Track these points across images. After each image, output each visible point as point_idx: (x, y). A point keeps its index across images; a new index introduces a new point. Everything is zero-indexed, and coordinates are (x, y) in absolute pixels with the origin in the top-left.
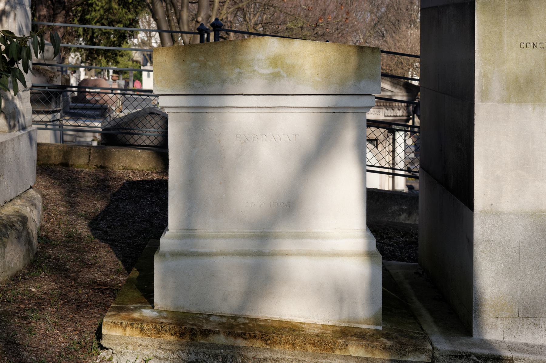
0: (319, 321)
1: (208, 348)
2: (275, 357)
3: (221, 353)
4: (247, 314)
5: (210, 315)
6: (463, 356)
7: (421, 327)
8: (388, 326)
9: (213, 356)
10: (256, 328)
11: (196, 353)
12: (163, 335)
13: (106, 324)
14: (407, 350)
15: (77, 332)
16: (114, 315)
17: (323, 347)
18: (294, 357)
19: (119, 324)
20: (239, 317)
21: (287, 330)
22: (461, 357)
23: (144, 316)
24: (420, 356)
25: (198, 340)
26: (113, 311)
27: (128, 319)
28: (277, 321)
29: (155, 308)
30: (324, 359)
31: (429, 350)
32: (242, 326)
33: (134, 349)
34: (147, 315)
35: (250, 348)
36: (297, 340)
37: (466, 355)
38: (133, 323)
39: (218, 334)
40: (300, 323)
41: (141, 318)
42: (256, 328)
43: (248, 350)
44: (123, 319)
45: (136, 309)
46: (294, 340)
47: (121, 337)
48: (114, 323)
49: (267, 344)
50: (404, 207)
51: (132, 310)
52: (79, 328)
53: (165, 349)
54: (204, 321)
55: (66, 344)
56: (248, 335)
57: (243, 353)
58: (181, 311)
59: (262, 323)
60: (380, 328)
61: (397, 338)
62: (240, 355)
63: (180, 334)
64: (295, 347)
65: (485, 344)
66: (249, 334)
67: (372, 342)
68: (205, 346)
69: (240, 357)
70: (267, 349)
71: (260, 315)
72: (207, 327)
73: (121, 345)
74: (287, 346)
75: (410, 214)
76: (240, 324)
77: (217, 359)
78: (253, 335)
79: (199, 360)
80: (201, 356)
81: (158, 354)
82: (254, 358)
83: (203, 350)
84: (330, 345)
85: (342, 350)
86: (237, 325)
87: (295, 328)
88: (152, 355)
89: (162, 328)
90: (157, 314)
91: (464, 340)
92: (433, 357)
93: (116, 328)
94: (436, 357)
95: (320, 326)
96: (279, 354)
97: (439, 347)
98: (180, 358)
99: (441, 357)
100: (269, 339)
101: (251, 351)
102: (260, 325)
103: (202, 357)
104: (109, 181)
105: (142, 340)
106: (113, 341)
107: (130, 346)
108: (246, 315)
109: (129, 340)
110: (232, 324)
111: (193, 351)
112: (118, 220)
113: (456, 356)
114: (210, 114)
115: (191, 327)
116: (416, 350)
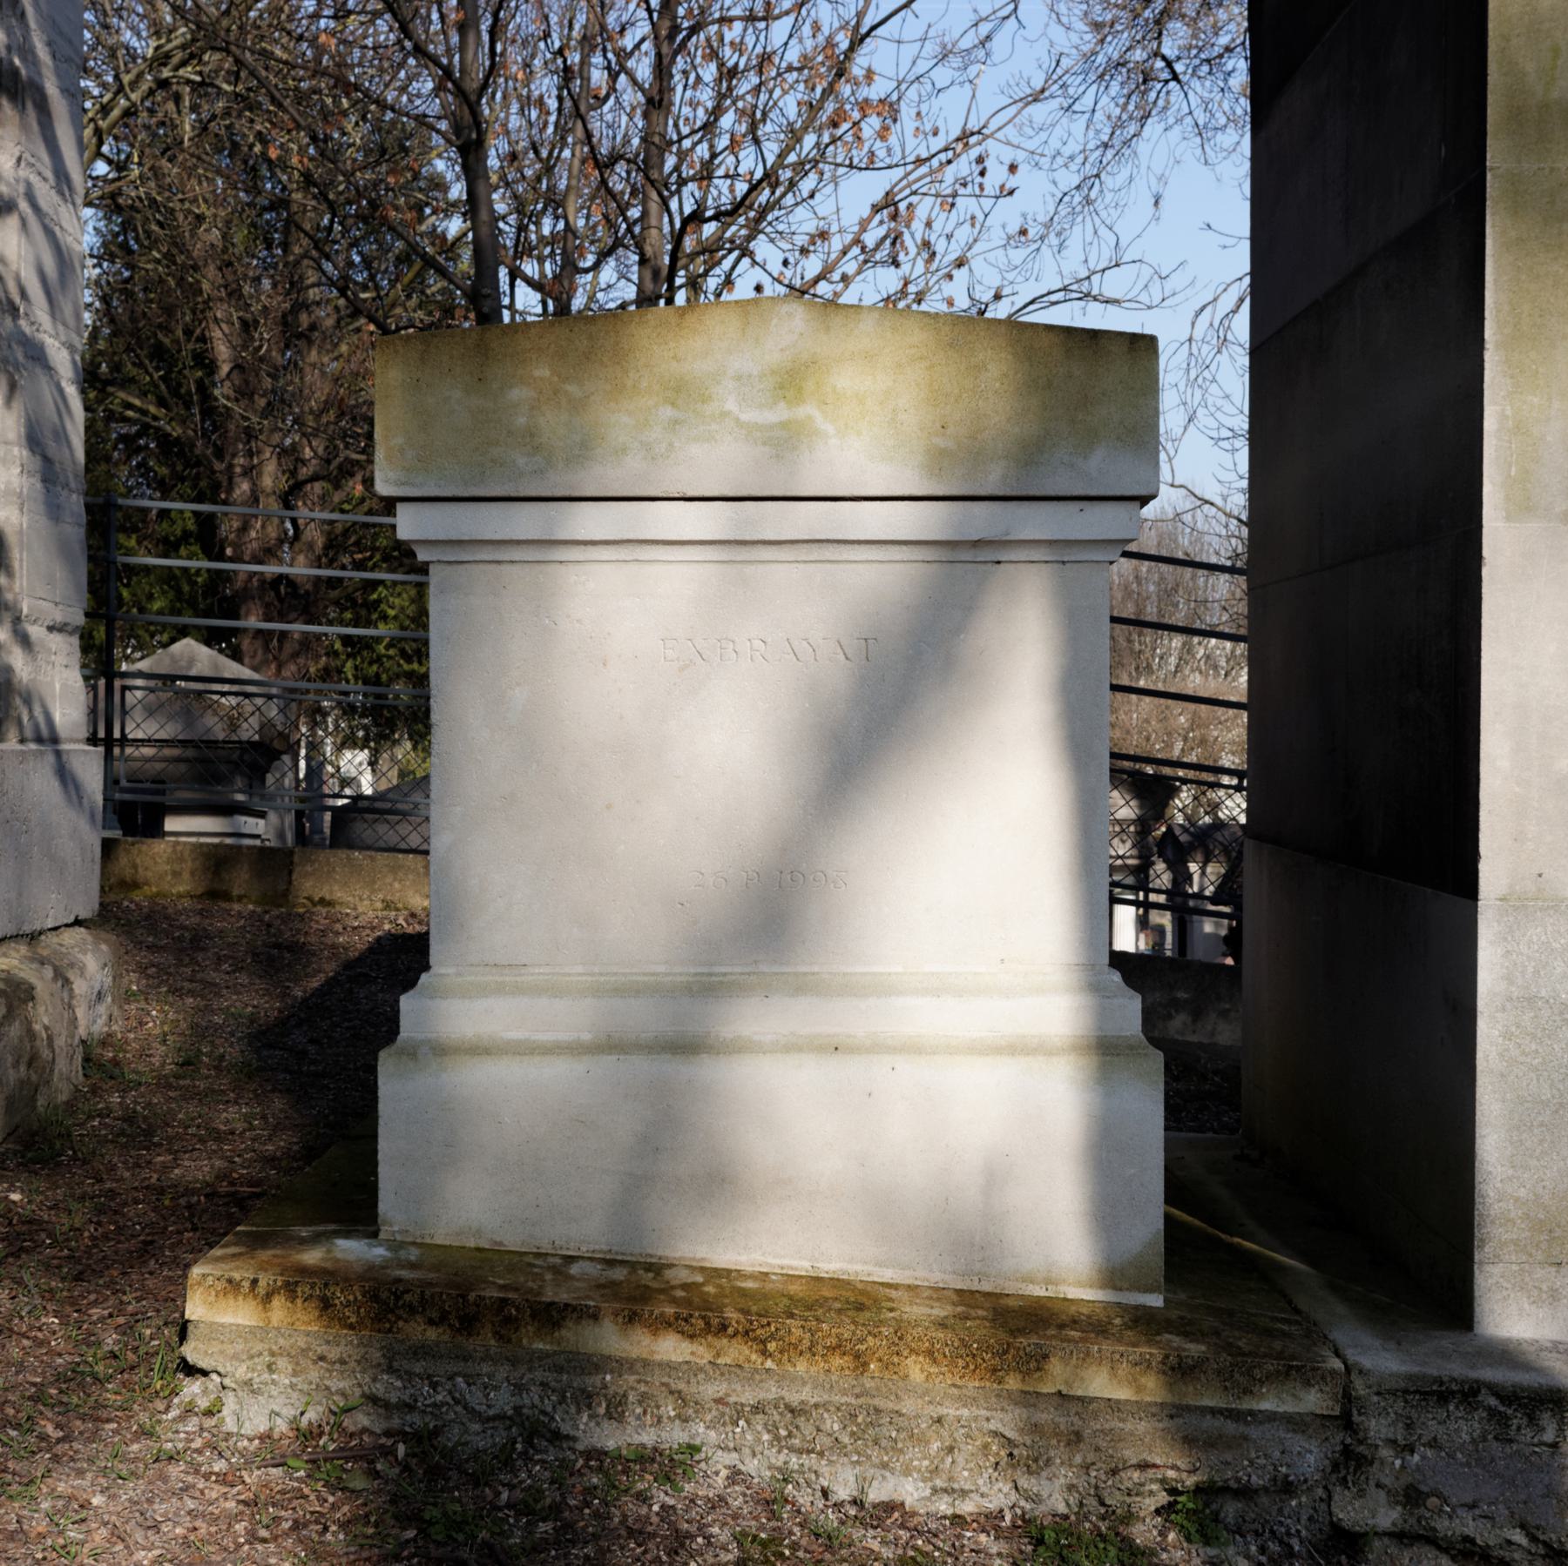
1: (560, 1369)
2: (794, 1398)
3: (605, 1387)
4: (699, 1255)
5: (570, 1259)
6: (1453, 1393)
7: (1290, 1302)
8: (1183, 1296)
10: (727, 1301)
11: (515, 1385)
12: (401, 1324)
13: (199, 1284)
14: (1257, 1373)
15: (121, 1320)
16: (234, 1255)
17: (961, 1363)
18: (861, 1401)
19: (246, 1284)
20: (671, 1266)
21: (837, 1305)
22: (1443, 1397)
23: (338, 1260)
24: (1302, 1394)
25: (525, 1341)
26: (236, 1244)
27: (278, 1270)
29: (382, 1236)
30: (965, 1406)
31: (1333, 1372)
32: (680, 1293)
33: (295, 1374)
34: (351, 1257)
35: (708, 1367)
36: (870, 1338)
37: (1462, 1392)
38: (297, 1283)
39: (595, 1317)
40: (882, 1284)
41: (328, 1265)
42: (727, 1301)
43: (701, 1376)
44: (262, 1268)
45: (315, 1239)
46: (862, 1341)
47: (252, 1330)
48: (230, 1281)
49: (765, 1353)
50: (1182, 995)
51: (303, 1242)
52: (130, 1308)
53: (406, 1372)
54: (549, 1277)
55: (68, 1358)
56: (701, 1323)
57: (681, 1386)
58: (472, 1245)
59: (750, 1284)
60: (1155, 1301)
61: (1217, 1333)
62: (672, 1393)
64: (865, 1365)
65: (1505, 1354)
66: (703, 1318)
70: (767, 1370)
71: (743, 1258)
72: (556, 1294)
73: (251, 1357)
74: (837, 1361)
75: (1197, 1014)
76: (673, 1288)
77: (589, 1407)
79: (525, 1411)
81: (379, 1389)
82: (718, 1401)
83: (539, 1375)
86: (662, 1291)
87: (864, 1300)
88: (358, 1392)
89: (398, 1298)
91: (1447, 1340)
92: (1347, 1398)
94: (1358, 1398)
95: (950, 1293)
96: (807, 1389)
97: (1366, 1362)
98: (457, 1402)
99: (1375, 1399)
100: (772, 1337)
101: (708, 1379)
102: (743, 1289)
104: (337, 934)
105: (328, 1342)
106: (225, 1346)
107: (282, 1363)
109: (282, 1341)
110: (647, 1287)
111: (507, 1379)
112: (348, 1028)
113: (1425, 1395)
115: (501, 1295)
116: (1287, 1374)
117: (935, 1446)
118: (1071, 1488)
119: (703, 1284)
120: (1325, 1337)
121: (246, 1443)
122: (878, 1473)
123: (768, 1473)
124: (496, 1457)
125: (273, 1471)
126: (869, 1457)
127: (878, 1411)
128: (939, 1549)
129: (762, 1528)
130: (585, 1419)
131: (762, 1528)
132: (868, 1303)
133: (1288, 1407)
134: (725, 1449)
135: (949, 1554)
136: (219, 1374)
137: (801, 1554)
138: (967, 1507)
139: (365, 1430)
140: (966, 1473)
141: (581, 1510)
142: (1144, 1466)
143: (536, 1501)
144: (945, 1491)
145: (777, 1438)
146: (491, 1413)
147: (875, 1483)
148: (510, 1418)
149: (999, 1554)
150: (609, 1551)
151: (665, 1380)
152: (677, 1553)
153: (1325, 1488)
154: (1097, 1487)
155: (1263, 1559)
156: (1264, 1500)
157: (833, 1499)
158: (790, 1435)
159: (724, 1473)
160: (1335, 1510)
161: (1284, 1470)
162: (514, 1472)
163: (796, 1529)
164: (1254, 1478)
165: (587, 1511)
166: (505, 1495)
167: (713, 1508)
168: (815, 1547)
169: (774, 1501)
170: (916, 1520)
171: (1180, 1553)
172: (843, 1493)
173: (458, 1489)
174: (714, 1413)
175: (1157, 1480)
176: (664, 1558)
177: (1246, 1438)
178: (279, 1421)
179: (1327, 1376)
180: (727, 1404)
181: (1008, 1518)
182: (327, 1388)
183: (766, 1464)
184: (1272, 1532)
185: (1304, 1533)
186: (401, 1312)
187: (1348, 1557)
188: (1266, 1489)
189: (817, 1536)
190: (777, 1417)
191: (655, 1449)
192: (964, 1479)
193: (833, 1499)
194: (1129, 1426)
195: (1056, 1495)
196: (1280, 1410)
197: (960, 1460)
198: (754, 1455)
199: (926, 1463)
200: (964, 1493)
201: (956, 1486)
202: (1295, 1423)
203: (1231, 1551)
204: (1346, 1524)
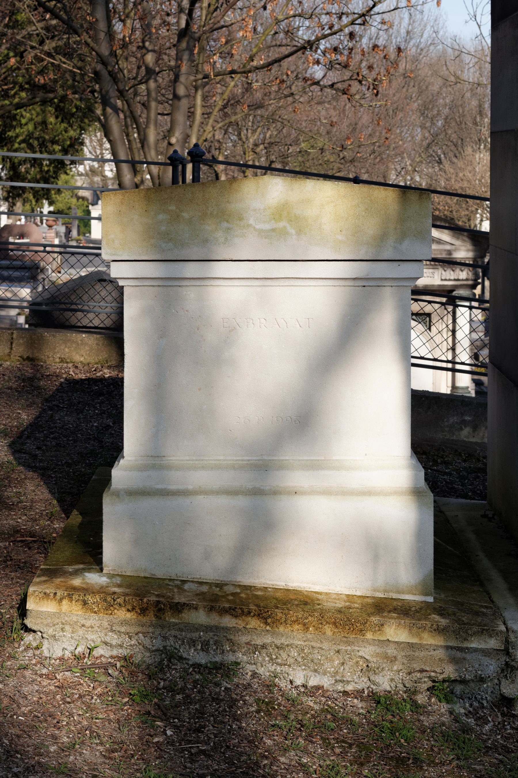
1: (181, 630)
3: (200, 637)
9: (188, 642)
10: (250, 601)
11: (163, 637)
12: (116, 611)
13: (32, 595)
14: (470, 632)
17: (347, 627)
18: (306, 643)
21: (296, 603)
23: (88, 584)
24: (488, 641)
25: (167, 619)
27: (64, 588)
28: (281, 589)
30: (349, 645)
31: (501, 632)
32: (231, 598)
33: (73, 632)
36: (310, 617)
38: (73, 594)
41: (84, 586)
42: (250, 601)
43: (240, 633)
44: (58, 587)
46: (306, 618)
47: (54, 614)
49: (266, 623)
54: (176, 590)
56: (240, 611)
57: (232, 637)
59: (260, 593)
60: (430, 599)
61: (454, 614)
62: (228, 640)
63: (140, 609)
66: (241, 609)
67: (419, 620)
68: (177, 626)
69: (227, 643)
70: (267, 631)
72: (180, 599)
73: (54, 625)
74: (296, 627)
76: (228, 595)
77: (194, 646)
79: (168, 648)
81: (108, 639)
82: (248, 643)
83: (173, 632)
85: (375, 632)
86: (223, 597)
88: (99, 640)
89: (114, 600)
92: (507, 642)
93: (47, 600)
95: (344, 596)
96: (284, 638)
98: (140, 644)
100: (269, 617)
101: (243, 634)
103: (172, 643)
105: (86, 619)
106: (43, 621)
108: (236, 582)
109: (66, 618)
110: (217, 595)
111: (160, 634)
115: (157, 599)
116: (482, 632)
117: (337, 662)
118: (392, 680)
119: (240, 593)
120: (501, 615)
121: (53, 661)
122: (313, 674)
123: (268, 674)
124: (156, 667)
125: (66, 673)
126: (309, 667)
127: (313, 647)
128: (337, 705)
129: (266, 697)
130: (192, 651)
131: (266, 697)
132: (309, 601)
133: (482, 646)
134: (250, 663)
135: (341, 708)
136: (41, 632)
137: (282, 708)
138: (349, 688)
139: (101, 656)
140: (349, 674)
141: (193, 690)
142: (422, 671)
143: (175, 686)
144: (340, 681)
145: (272, 659)
146: (154, 648)
147: (312, 678)
148: (162, 651)
149: (362, 708)
150: (205, 707)
151: (225, 634)
152: (232, 708)
153: (498, 679)
154: (402, 680)
155: (471, 709)
156: (472, 685)
157: (295, 684)
158: (277, 658)
159: (250, 673)
160: (502, 688)
161: (480, 672)
162: (165, 674)
163: (280, 698)
164: (467, 676)
165: (195, 690)
166: (162, 684)
167: (246, 688)
168: (287, 705)
169: (271, 686)
170: (328, 693)
171: (436, 707)
172: (299, 682)
173: (142, 681)
174: (246, 648)
175: (427, 677)
176: (227, 709)
177: (464, 659)
178: (66, 652)
179: (498, 633)
180: (251, 645)
181: (366, 692)
182: (87, 638)
183: (267, 670)
184: (476, 698)
185: (489, 698)
186: (115, 606)
187: (507, 708)
188: (473, 681)
189: (288, 700)
190: (271, 651)
191: (221, 664)
192: (348, 677)
193: (295, 684)
194: (417, 654)
195: (386, 683)
196: (479, 647)
197: (347, 668)
198: (262, 666)
199: (333, 669)
200: (348, 682)
201: (345, 679)
202: (486, 653)
203: (458, 705)
204: (506, 695)
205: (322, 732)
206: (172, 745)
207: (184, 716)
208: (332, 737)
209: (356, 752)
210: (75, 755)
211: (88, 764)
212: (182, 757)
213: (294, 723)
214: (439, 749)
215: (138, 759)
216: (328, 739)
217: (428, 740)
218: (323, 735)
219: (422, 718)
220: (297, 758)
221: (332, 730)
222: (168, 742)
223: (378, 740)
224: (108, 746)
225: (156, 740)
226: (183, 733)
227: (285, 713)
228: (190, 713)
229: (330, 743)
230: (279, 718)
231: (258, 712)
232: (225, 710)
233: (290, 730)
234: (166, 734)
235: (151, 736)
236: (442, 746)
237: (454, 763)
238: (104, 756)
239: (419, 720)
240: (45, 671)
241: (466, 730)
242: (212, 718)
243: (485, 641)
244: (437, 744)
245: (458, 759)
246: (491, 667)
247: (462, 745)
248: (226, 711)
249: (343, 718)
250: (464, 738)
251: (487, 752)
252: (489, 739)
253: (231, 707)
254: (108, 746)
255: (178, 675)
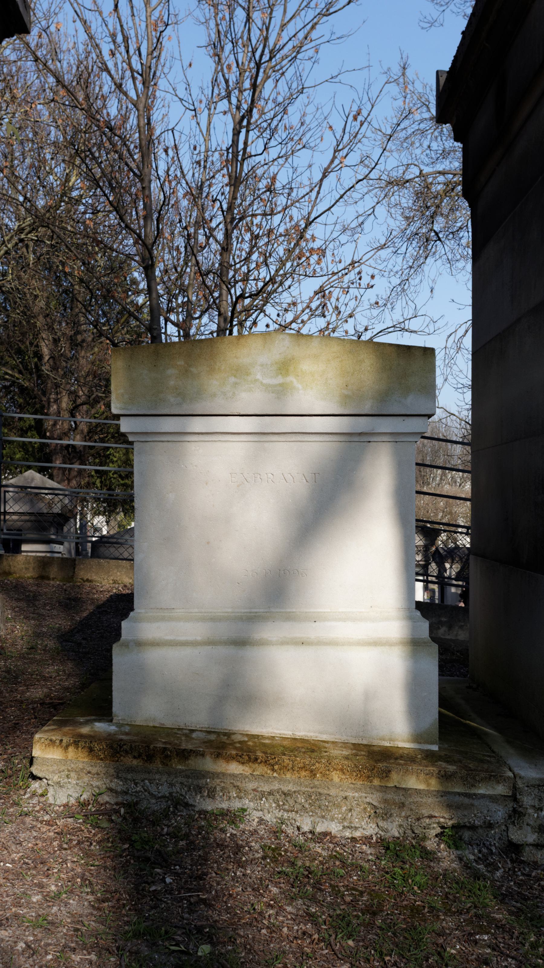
0: (348, 738)
1: (188, 777)
2: (285, 789)
3: (207, 784)
4: (246, 729)
5: (192, 731)
7: (490, 748)
8: (446, 746)
9: (194, 788)
11: (170, 784)
13: (38, 741)
14: (477, 778)
15: (5, 756)
16: (53, 730)
17: (355, 774)
18: (313, 790)
19: (58, 742)
20: (234, 734)
21: (303, 750)
23: (96, 732)
24: (496, 787)
25: (174, 765)
26: (53, 725)
28: (288, 738)
29: (114, 721)
30: (356, 792)
31: (509, 778)
32: (238, 745)
33: (78, 779)
34: (101, 730)
35: (250, 776)
36: (317, 764)
38: (79, 741)
39: (203, 755)
40: (322, 741)
41: (92, 734)
43: (247, 780)
44: (65, 735)
45: (87, 723)
46: (314, 765)
47: (60, 761)
48: (51, 740)
49: (273, 770)
51: (81, 724)
52: (9, 751)
53: (124, 778)
54: (183, 738)
56: (247, 758)
57: (239, 784)
59: (267, 741)
60: (435, 748)
61: (460, 761)
62: (235, 787)
63: (147, 756)
66: (248, 755)
67: (426, 766)
68: (184, 773)
69: (234, 789)
70: (274, 777)
71: (264, 730)
73: (60, 772)
74: (303, 773)
76: (235, 743)
77: (200, 792)
78: (253, 757)
79: (174, 794)
80: (177, 788)
81: (113, 785)
82: (254, 790)
83: (180, 779)
84: (365, 771)
86: (230, 744)
87: (315, 748)
88: (104, 786)
89: (121, 747)
90: (116, 729)
92: (515, 788)
93: (53, 747)
96: (291, 785)
97: (522, 773)
98: (146, 791)
99: (526, 788)
100: (276, 763)
101: (250, 781)
102: (265, 743)
103: (178, 790)
104: (94, 594)
105: (92, 766)
106: (49, 768)
107: (73, 774)
109: (72, 765)
110: (224, 743)
111: (166, 781)
114: (193, 443)
116: (490, 779)
117: (344, 808)
118: (400, 826)
119: (247, 741)
120: (505, 763)
121: (58, 808)
122: (320, 820)
123: (275, 820)
124: (162, 814)
125: (69, 820)
126: (317, 813)
127: (320, 794)
128: (346, 852)
129: (272, 843)
130: (199, 798)
132: (316, 749)
133: (490, 792)
134: (257, 810)
135: (350, 854)
136: (46, 779)
137: (289, 854)
138: (357, 834)
139: (107, 802)
140: (357, 820)
141: (197, 836)
142: (431, 817)
143: (179, 832)
144: (348, 827)
145: (278, 805)
146: (160, 795)
147: (319, 824)
148: (167, 797)
149: (371, 854)
150: (209, 853)
151: (232, 781)
152: (237, 854)
153: (506, 825)
154: (411, 826)
155: (480, 855)
156: (480, 831)
157: (302, 831)
158: (284, 804)
159: (256, 820)
160: (510, 835)
161: (488, 818)
162: (170, 820)
164: (476, 822)
165: (200, 836)
167: (252, 835)
168: (294, 851)
169: (277, 832)
170: (336, 840)
171: (446, 853)
172: (306, 828)
173: (146, 827)
174: (252, 795)
175: (436, 823)
176: (232, 856)
177: (472, 805)
178: (71, 799)
180: (257, 791)
181: (374, 838)
182: (92, 785)
183: (274, 816)
184: (484, 844)
185: (497, 844)
186: (122, 753)
187: (515, 854)
188: (481, 826)
189: (295, 846)
190: (278, 797)
191: (228, 810)
192: (356, 822)
193: (302, 831)
194: (424, 800)
195: (394, 829)
196: (487, 793)
197: (355, 814)
198: (269, 813)
199: (340, 816)
200: (356, 828)
201: (353, 825)
202: (493, 799)
203: (467, 852)
204: (515, 841)
205: (331, 879)
206: (170, 894)
207: (186, 863)
208: (342, 884)
209: (368, 901)
210: (59, 905)
211: (73, 915)
212: (180, 907)
213: (301, 870)
214: (454, 897)
215: (130, 909)
216: (337, 886)
217: (442, 887)
218: (332, 882)
219: (432, 864)
220: (304, 907)
221: (341, 876)
222: (166, 891)
223: (390, 888)
224: (99, 895)
225: (153, 888)
226: (183, 880)
227: (292, 860)
228: (192, 860)
229: (339, 891)
230: (286, 865)
231: (264, 858)
232: (229, 857)
233: (297, 877)
234: (165, 882)
235: (149, 884)
236: (457, 893)
237: (473, 911)
238: (93, 906)
239: (430, 867)
240: (46, 818)
241: (477, 876)
242: (215, 865)
243: (493, 787)
244: (451, 891)
245: (476, 907)
246: (500, 813)
247: (478, 892)
248: (231, 858)
249: (352, 864)
250: (479, 885)
251: (504, 899)
252: (503, 886)
253: (236, 853)
254: (99, 895)
255: (183, 821)
